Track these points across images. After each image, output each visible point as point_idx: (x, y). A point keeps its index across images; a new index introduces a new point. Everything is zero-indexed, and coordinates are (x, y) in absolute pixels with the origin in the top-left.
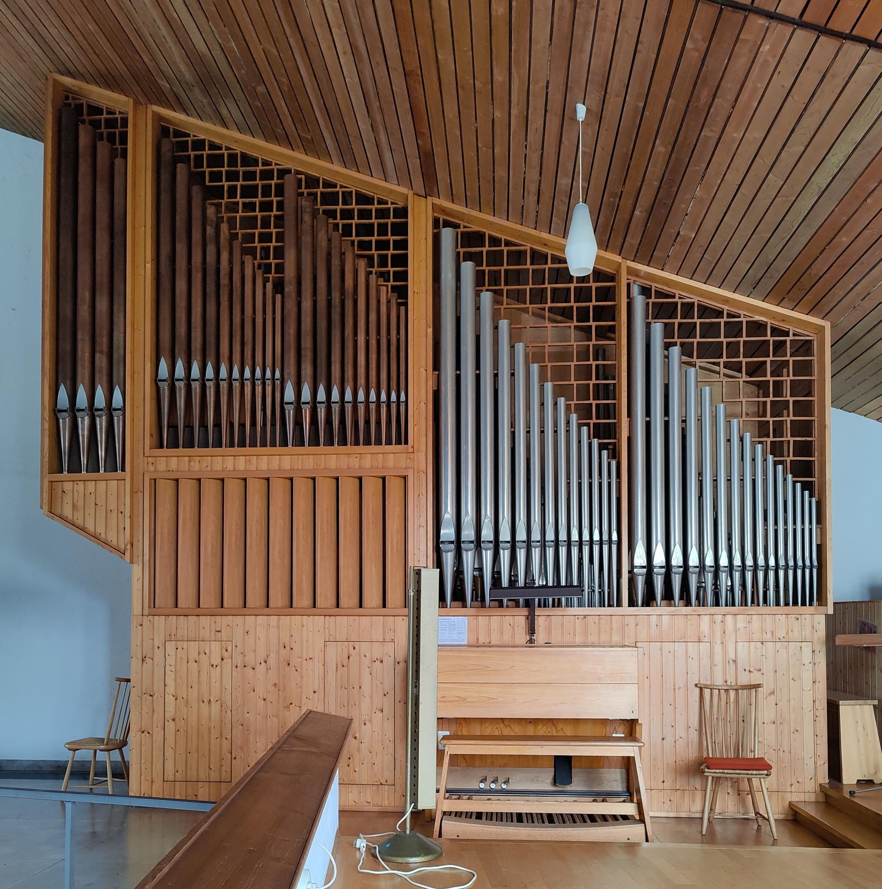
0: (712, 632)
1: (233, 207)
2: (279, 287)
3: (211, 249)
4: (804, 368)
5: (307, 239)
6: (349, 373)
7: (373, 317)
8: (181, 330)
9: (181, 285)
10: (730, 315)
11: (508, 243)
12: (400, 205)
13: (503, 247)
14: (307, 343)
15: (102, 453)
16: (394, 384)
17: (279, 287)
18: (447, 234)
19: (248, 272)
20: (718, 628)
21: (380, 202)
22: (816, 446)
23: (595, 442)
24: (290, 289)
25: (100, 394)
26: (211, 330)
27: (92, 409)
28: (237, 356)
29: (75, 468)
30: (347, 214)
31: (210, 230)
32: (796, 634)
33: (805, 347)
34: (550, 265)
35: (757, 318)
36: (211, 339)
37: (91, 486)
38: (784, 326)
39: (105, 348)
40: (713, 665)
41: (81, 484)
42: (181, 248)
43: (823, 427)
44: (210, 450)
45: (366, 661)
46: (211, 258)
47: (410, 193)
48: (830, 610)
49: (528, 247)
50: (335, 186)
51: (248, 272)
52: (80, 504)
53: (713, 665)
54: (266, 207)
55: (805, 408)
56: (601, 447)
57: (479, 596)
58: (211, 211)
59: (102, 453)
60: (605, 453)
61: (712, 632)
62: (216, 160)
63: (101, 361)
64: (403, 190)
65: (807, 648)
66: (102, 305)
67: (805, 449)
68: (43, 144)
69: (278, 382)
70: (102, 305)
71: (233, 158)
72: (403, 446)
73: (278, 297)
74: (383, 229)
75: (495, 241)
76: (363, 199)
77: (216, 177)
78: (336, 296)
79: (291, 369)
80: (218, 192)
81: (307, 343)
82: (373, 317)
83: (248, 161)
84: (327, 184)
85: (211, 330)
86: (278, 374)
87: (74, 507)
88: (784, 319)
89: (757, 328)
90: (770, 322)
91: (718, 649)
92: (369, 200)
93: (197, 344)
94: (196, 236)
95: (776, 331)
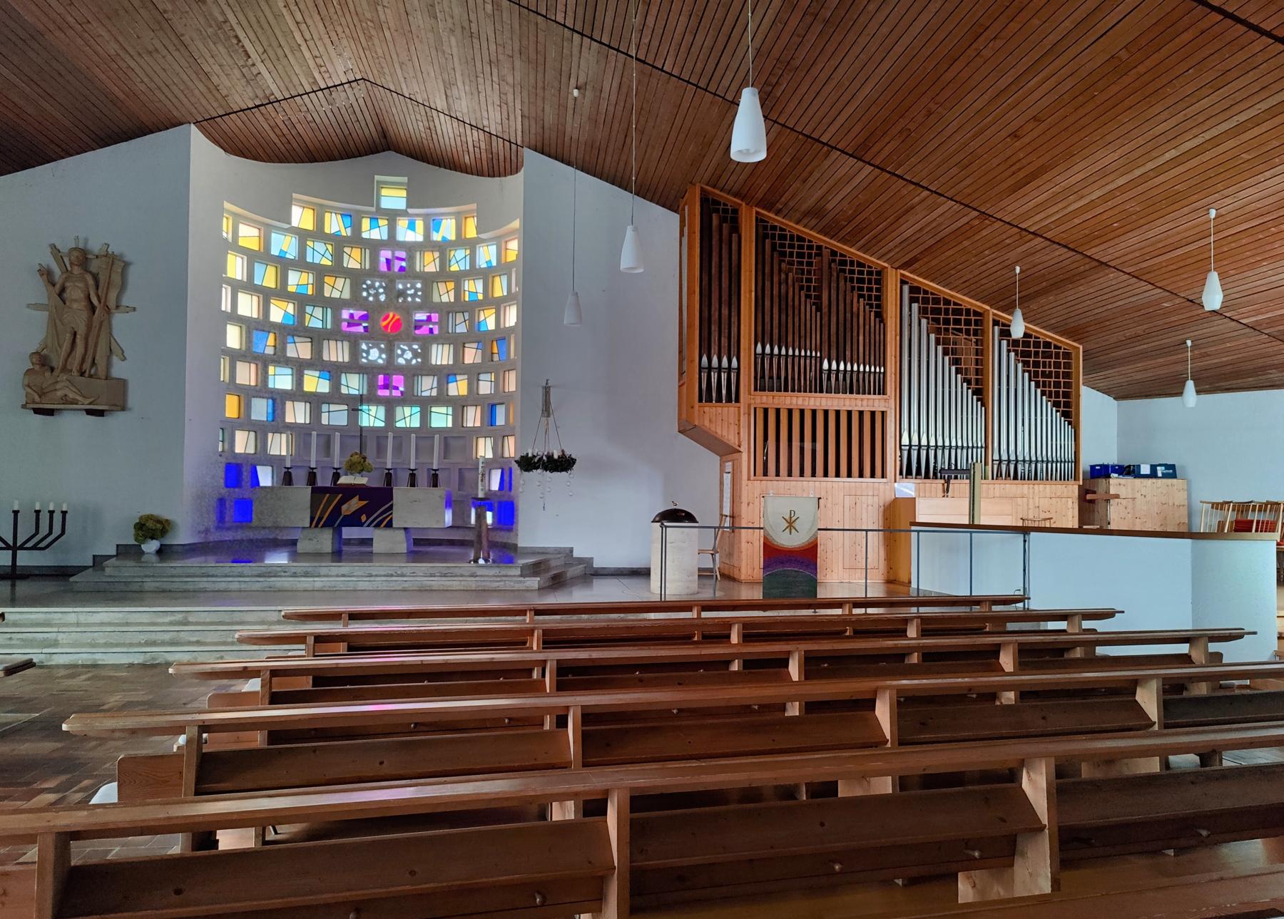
0: (1029, 493)
1: (791, 263)
2: (819, 309)
3: (783, 287)
4: (1068, 365)
5: (834, 285)
6: (855, 357)
7: (867, 327)
8: (768, 327)
9: (767, 303)
10: (1036, 337)
11: (932, 294)
12: (879, 269)
13: (929, 296)
14: (833, 338)
15: (724, 392)
16: (877, 362)
17: (819, 309)
18: (906, 288)
19: (803, 299)
20: (1031, 491)
21: (869, 267)
22: (1073, 404)
23: (975, 397)
24: (825, 310)
25: (725, 360)
26: (783, 329)
27: (720, 369)
28: (797, 344)
29: (709, 400)
30: (852, 272)
31: (783, 276)
32: (1065, 495)
33: (1067, 355)
34: (952, 306)
35: (1048, 340)
36: (783, 333)
37: (719, 410)
38: (1059, 345)
39: (727, 335)
40: (1029, 509)
41: (714, 409)
42: (768, 284)
43: (1078, 396)
44: (783, 393)
45: (865, 506)
46: (783, 291)
47: (889, 267)
48: (1081, 483)
49: (942, 296)
50: (846, 256)
51: (803, 299)
52: (714, 419)
53: (1029, 509)
54: (809, 264)
55: (1068, 385)
56: (978, 400)
57: (918, 473)
58: (783, 265)
59: (724, 392)
60: (979, 403)
61: (1029, 493)
62: (783, 237)
63: (724, 341)
64: (886, 265)
65: (1070, 501)
66: (725, 312)
67: (1067, 405)
68: (676, 217)
69: (818, 359)
70: (725, 312)
71: (792, 237)
72: (881, 396)
73: (818, 314)
74: (870, 281)
75: (926, 292)
76: (860, 264)
77: (783, 246)
78: (848, 315)
79: (825, 352)
80: (783, 254)
81: (833, 338)
82: (867, 327)
83: (801, 239)
84: (842, 255)
85: (783, 329)
86: (818, 355)
87: (710, 421)
88: (1061, 342)
89: (1047, 345)
90: (1053, 342)
91: (1031, 500)
92: (863, 265)
93: (776, 337)
94: (776, 279)
95: (1056, 347)
